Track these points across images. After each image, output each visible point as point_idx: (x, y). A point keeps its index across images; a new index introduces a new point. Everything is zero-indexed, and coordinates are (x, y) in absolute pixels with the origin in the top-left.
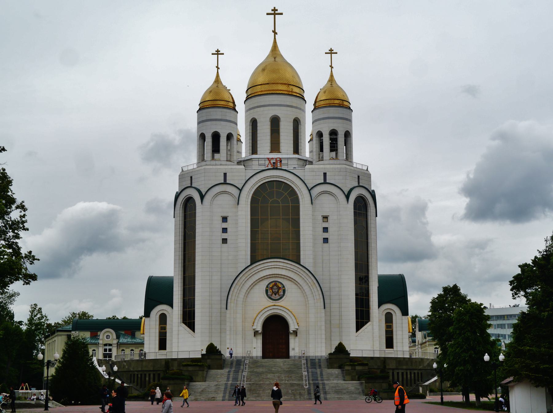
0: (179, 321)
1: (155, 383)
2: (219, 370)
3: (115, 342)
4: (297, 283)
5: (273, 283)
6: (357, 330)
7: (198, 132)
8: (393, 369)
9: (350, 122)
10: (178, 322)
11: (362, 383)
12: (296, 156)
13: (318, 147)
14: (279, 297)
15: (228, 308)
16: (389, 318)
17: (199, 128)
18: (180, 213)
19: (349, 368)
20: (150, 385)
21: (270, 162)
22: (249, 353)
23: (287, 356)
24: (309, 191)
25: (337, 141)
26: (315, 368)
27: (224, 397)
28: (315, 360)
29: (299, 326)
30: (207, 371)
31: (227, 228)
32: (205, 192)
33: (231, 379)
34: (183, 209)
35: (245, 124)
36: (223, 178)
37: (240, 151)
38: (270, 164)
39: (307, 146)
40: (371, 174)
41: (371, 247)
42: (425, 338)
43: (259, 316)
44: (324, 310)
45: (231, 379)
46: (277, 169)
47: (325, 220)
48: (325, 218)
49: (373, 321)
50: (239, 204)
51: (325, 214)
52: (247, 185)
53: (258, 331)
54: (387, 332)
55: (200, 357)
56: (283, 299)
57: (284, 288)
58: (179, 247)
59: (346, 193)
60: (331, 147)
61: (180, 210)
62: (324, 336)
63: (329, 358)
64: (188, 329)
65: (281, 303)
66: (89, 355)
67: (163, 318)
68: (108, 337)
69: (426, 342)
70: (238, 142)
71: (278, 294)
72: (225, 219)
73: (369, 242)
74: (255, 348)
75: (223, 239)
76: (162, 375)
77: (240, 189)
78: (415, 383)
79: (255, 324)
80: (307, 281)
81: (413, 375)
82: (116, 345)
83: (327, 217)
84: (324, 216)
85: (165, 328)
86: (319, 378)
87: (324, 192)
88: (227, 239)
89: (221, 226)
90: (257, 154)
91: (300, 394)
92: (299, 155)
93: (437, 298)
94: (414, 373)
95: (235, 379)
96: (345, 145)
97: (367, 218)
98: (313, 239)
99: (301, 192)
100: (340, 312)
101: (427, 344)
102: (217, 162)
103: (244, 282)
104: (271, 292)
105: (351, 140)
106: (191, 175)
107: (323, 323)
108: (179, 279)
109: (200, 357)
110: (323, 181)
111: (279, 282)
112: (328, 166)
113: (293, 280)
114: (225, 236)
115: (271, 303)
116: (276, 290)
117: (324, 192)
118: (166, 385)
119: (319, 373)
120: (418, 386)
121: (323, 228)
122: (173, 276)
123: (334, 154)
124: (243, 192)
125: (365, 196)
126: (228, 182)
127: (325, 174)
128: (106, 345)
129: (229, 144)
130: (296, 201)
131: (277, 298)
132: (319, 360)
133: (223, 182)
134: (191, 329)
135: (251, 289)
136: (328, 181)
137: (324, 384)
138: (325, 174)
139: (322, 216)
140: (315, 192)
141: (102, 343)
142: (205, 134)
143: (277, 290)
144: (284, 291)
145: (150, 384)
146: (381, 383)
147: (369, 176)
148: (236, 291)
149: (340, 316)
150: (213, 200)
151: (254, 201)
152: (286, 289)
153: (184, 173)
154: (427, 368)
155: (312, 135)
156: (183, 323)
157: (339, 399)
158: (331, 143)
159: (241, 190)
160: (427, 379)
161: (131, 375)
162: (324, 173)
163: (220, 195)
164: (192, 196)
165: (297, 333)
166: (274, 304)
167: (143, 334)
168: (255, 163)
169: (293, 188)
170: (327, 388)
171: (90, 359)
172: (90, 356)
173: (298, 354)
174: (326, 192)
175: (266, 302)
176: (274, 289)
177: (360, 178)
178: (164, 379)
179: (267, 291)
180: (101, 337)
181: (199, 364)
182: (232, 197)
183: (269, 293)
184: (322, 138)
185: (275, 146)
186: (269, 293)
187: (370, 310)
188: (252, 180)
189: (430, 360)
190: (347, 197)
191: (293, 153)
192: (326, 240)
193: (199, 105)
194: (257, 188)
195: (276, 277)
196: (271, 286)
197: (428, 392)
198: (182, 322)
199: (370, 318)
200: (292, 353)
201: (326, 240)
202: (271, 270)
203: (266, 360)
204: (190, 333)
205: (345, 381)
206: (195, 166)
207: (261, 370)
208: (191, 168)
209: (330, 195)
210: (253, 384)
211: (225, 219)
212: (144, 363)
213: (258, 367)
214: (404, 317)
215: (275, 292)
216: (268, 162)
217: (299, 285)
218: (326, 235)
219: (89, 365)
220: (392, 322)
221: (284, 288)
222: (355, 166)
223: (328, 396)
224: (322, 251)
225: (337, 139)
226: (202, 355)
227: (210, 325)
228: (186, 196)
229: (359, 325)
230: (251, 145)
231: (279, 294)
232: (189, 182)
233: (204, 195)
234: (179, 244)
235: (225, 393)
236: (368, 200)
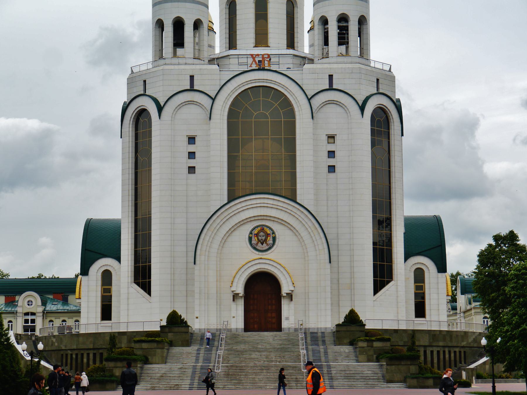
0: (130, 281)
1: (95, 366)
2: (184, 348)
3: (40, 309)
4: (292, 228)
5: (259, 228)
6: (376, 292)
7: (153, 18)
8: (425, 346)
9: (367, 2)
10: (128, 282)
11: (382, 365)
12: (291, 51)
13: (321, 38)
14: (267, 247)
15: (197, 262)
17: (154, 13)
18: (129, 131)
19: (364, 344)
20: (90, 368)
21: (254, 60)
23: (279, 328)
24: (309, 100)
25: (347, 30)
26: (317, 345)
27: (191, 384)
28: (317, 333)
29: (294, 287)
30: (168, 349)
31: (194, 153)
32: (164, 103)
33: (201, 360)
34: (134, 126)
35: (220, 6)
37: (212, 45)
38: (254, 63)
39: (306, 36)
40: (395, 77)
41: (395, 177)
42: (470, 303)
43: (240, 273)
44: (329, 264)
45: (201, 360)
46: (264, 69)
47: (331, 140)
48: (331, 138)
49: (397, 280)
50: (211, 118)
51: (331, 133)
52: (222, 92)
53: (238, 294)
54: (416, 294)
55: (159, 329)
56: (272, 249)
57: (274, 235)
58: (129, 179)
59: (360, 104)
60: (339, 38)
61: (129, 127)
62: (329, 301)
63: (337, 331)
64: (142, 291)
66: (3, 328)
68: (30, 303)
69: (471, 310)
70: (210, 32)
71: (266, 243)
72: (192, 140)
73: (391, 171)
74: (234, 317)
75: (189, 167)
76: (105, 355)
77: (213, 96)
78: (456, 366)
79: (235, 284)
80: (306, 225)
81: (452, 355)
82: (41, 314)
83: (334, 137)
84: (330, 136)
85: (109, 291)
86: (323, 359)
87: (330, 102)
88: (194, 167)
89: (187, 149)
90: (236, 49)
91: (297, 380)
92: (294, 50)
93: (486, 250)
94: (455, 352)
95: (207, 360)
96: (360, 36)
97: (389, 138)
98: (314, 167)
99: (297, 101)
100: (352, 267)
101: (473, 311)
102: (181, 61)
103: (219, 226)
104: (256, 240)
105: (368, 29)
106: (144, 79)
107: (328, 283)
108: (129, 222)
109: (159, 329)
110: (328, 87)
111: (268, 227)
112: (335, 66)
113: (286, 224)
114: (192, 163)
115: (256, 255)
116: (264, 238)
117: (330, 102)
118: (111, 368)
119: (322, 350)
120: (460, 369)
121: (329, 152)
122: (121, 218)
123: (343, 48)
124: (217, 101)
125: (386, 107)
126: (195, 88)
127: (331, 77)
128: (27, 314)
129: (197, 35)
131: (265, 249)
132: (323, 333)
133: (189, 88)
134: (145, 291)
135: (229, 236)
136: (334, 87)
137: (329, 367)
138: (331, 77)
139: (326, 135)
141: (22, 312)
142: (163, 20)
143: (264, 237)
145: (89, 367)
146: (408, 365)
147: (392, 79)
148: (207, 238)
149: (352, 273)
150: (175, 112)
151: (232, 114)
152: (277, 236)
153: (134, 75)
154: (472, 345)
155: (313, 22)
156: (135, 283)
157: (351, 387)
158: (339, 34)
159: (214, 100)
160: (472, 361)
161: (62, 355)
162: (329, 75)
163: (185, 107)
164: (146, 108)
165: (292, 296)
167: (80, 298)
168: (234, 61)
169: (286, 96)
170: (333, 372)
171: (5, 333)
172: (4, 329)
173: (293, 325)
174: (332, 102)
176: (260, 236)
177: (380, 81)
178: (107, 360)
179: (250, 239)
180: (20, 304)
181: (157, 339)
182: (201, 109)
183: (254, 241)
184: (326, 27)
186: (253, 242)
187: (393, 265)
188: (229, 84)
189: (478, 334)
190: (362, 108)
191: (286, 47)
194: (236, 96)
195: (264, 219)
196: (256, 232)
197: (474, 378)
199: (394, 276)
200: (285, 324)
202: (255, 210)
203: (249, 333)
204: (144, 297)
205: (358, 362)
206: (150, 66)
207: (241, 347)
208: (143, 68)
209: (337, 106)
210: (232, 366)
211: (192, 140)
212: (81, 339)
213: (237, 343)
214: (440, 274)
215: (262, 239)
216: (252, 60)
217: (294, 230)
218: (331, 162)
219: (3, 342)
220: (423, 282)
221: (274, 235)
222: (372, 64)
223: (335, 383)
224: (327, 184)
225: (347, 27)
226: (161, 327)
227: (172, 286)
228: (138, 107)
229: (378, 286)
230: (228, 36)
231: (268, 243)
232: (142, 88)
233: (162, 106)
234: (129, 174)
235: (193, 378)
236: (390, 112)
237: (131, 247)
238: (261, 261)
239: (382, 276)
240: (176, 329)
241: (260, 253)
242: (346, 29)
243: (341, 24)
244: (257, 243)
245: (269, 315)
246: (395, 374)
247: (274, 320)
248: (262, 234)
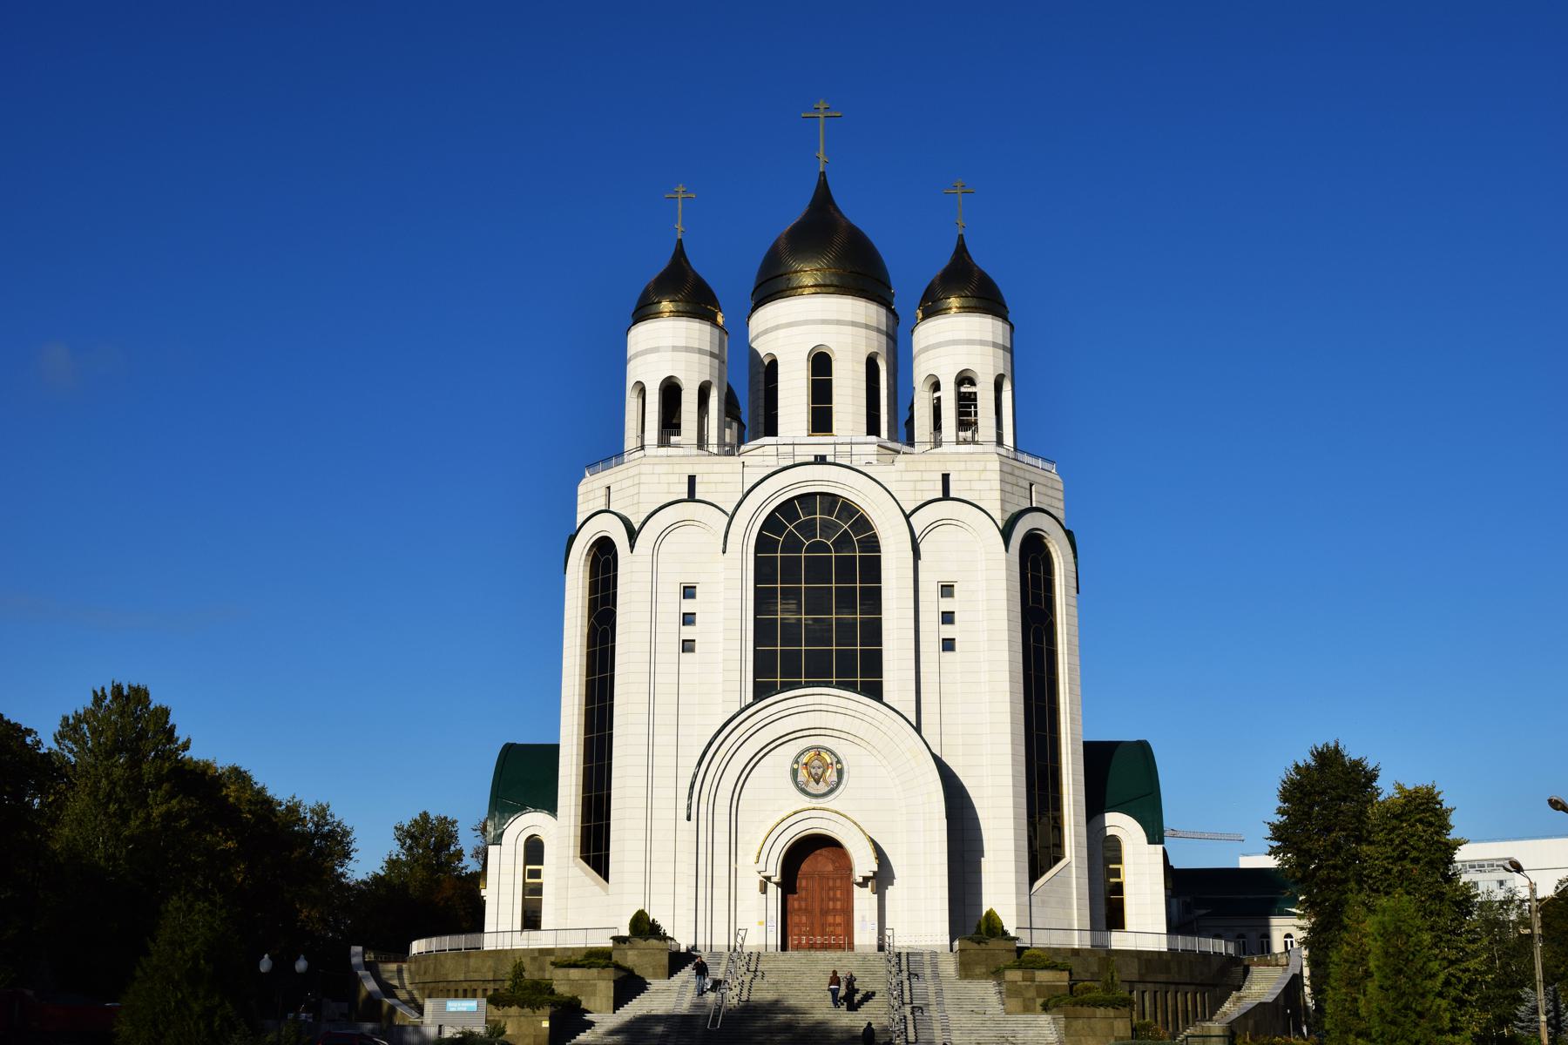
12: (873, 438)
14: (827, 789)
22: (743, 935)
24: (907, 517)
25: (975, 400)
28: (921, 954)
36: (685, 488)
56: (837, 793)
57: (839, 766)
67: (534, 850)
71: (825, 781)
72: (689, 592)
106: (607, 484)
109: (610, 944)
110: (941, 496)
111: (828, 750)
114: (688, 632)
115: (806, 802)
134: (600, 874)
140: (919, 521)
144: (840, 773)
156: (581, 857)
162: (943, 475)
166: (812, 806)
179: (795, 773)
183: (803, 775)
184: (936, 395)
185: (821, 421)
186: (799, 779)
190: (1006, 534)
192: (948, 645)
193: (633, 315)
196: (805, 761)
198: (579, 855)
211: (689, 592)
215: (816, 774)
221: (839, 766)
233: (637, 528)
237: (577, 791)
238: (813, 814)
240: (641, 943)
241: (815, 803)
242: (973, 397)
243: (963, 389)
245: (830, 919)
247: (839, 930)
248: (817, 763)
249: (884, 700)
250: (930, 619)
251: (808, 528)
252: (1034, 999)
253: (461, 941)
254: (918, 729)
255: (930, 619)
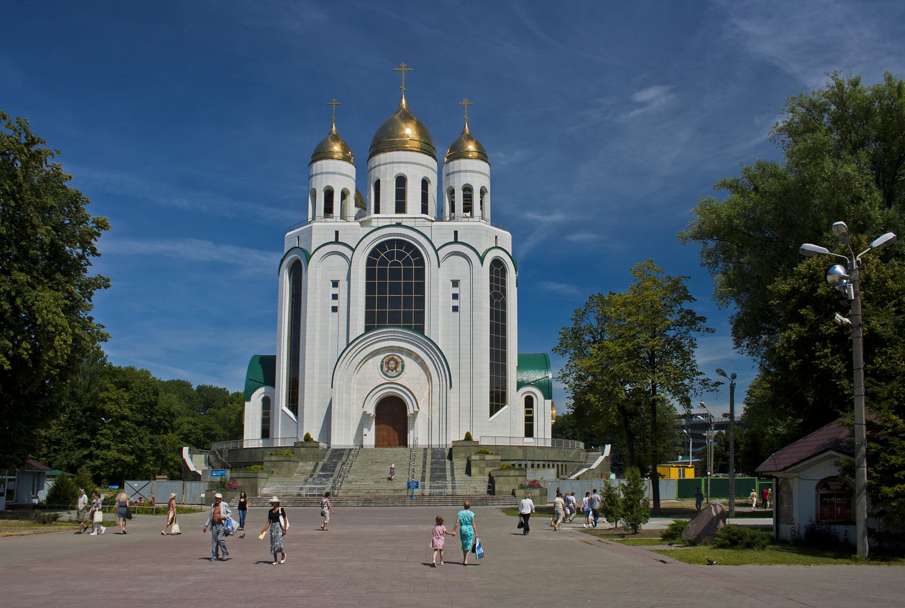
6: (492, 413)
12: (424, 215)
14: (397, 374)
16: (529, 402)
24: (436, 251)
56: (401, 376)
65: (399, 380)
116: (394, 366)
127: (456, 233)
130: (421, 262)
133: (334, 240)
138: (456, 233)
140: (442, 253)
159: (353, 250)
175: (381, 379)
177: (498, 238)
185: (401, 207)
186: (384, 369)
190: (482, 259)
192: (455, 309)
200: (410, 442)
201: (455, 309)
218: (456, 303)
220: (532, 407)
229: (493, 410)
239: (497, 401)
241: (391, 379)
244: (388, 371)
246: (504, 486)
248: (392, 362)
249: (426, 334)
250: (343, 296)
251: (390, 255)
252: (484, 468)
253: (231, 445)
254: (348, 345)
255: (343, 296)
